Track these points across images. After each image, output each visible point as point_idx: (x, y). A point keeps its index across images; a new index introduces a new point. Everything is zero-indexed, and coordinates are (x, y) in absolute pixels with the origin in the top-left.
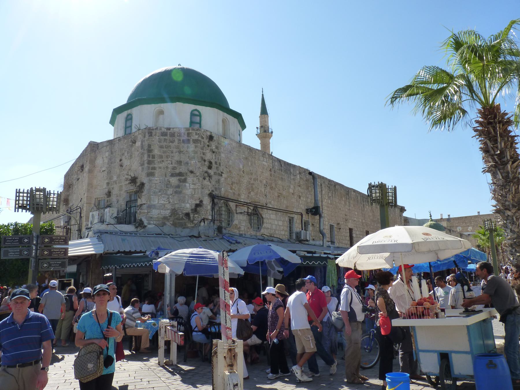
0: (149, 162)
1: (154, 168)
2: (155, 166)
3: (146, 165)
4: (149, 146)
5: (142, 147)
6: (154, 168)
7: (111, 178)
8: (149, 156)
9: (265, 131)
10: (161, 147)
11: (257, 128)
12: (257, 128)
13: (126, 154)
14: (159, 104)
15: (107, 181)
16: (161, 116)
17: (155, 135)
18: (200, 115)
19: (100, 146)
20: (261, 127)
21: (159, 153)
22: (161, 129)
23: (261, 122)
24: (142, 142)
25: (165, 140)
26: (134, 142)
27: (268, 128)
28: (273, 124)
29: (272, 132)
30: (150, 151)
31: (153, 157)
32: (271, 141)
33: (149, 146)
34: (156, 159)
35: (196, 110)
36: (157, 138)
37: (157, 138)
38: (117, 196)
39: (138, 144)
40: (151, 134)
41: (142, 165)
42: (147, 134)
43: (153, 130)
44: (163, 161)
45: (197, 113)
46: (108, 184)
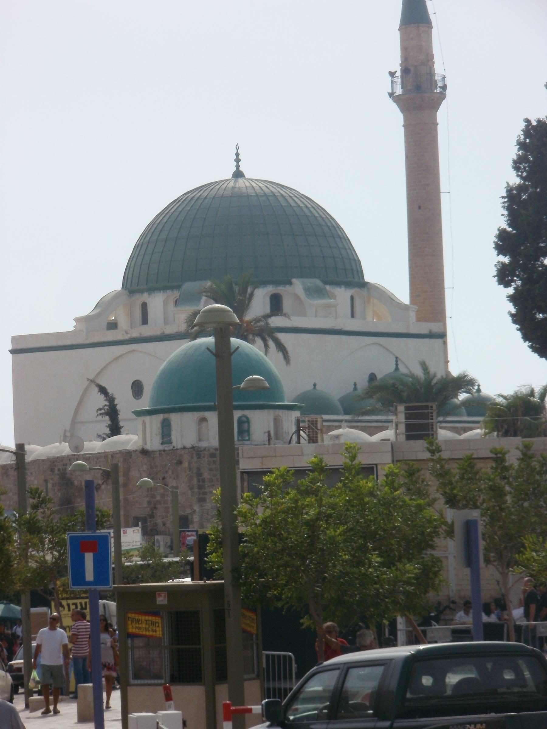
0: (200, 487)
1: (205, 493)
2: (207, 490)
3: (196, 490)
4: (199, 469)
5: (190, 469)
6: (205, 493)
7: (153, 496)
8: (198, 480)
9: (418, 88)
10: (211, 470)
11: (392, 74)
12: (392, 74)
13: (170, 472)
14: (202, 412)
15: (148, 499)
16: (204, 424)
17: (204, 457)
18: (248, 421)
19: (134, 455)
20: (405, 71)
21: (209, 477)
22: (209, 450)
23: (405, 50)
24: (190, 463)
25: (214, 461)
26: (180, 463)
27: (431, 74)
28: (447, 59)
29: (444, 87)
30: (199, 474)
31: (203, 480)
32: (443, 115)
33: (199, 469)
34: (206, 483)
35: (244, 416)
36: (206, 460)
37: (206, 460)
38: (163, 518)
39: (186, 464)
40: (199, 456)
41: (191, 489)
42: (195, 455)
43: (201, 451)
44: (213, 485)
45: (245, 419)
46: (149, 502)
